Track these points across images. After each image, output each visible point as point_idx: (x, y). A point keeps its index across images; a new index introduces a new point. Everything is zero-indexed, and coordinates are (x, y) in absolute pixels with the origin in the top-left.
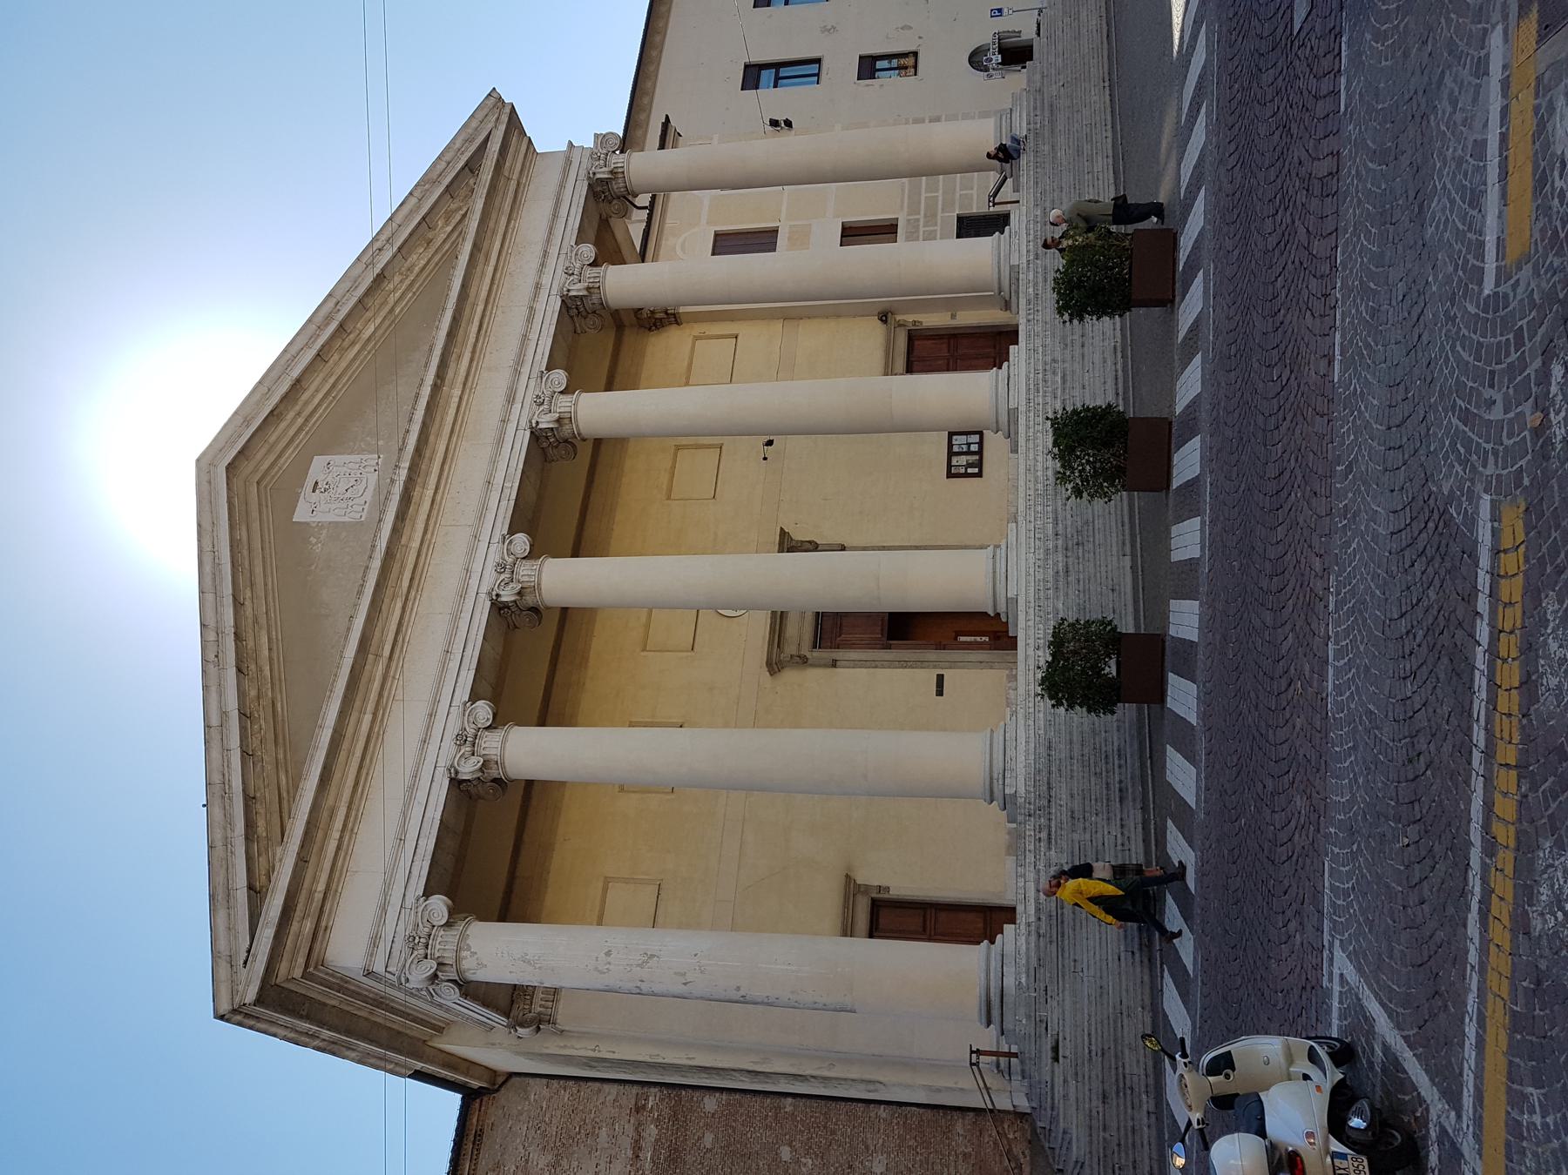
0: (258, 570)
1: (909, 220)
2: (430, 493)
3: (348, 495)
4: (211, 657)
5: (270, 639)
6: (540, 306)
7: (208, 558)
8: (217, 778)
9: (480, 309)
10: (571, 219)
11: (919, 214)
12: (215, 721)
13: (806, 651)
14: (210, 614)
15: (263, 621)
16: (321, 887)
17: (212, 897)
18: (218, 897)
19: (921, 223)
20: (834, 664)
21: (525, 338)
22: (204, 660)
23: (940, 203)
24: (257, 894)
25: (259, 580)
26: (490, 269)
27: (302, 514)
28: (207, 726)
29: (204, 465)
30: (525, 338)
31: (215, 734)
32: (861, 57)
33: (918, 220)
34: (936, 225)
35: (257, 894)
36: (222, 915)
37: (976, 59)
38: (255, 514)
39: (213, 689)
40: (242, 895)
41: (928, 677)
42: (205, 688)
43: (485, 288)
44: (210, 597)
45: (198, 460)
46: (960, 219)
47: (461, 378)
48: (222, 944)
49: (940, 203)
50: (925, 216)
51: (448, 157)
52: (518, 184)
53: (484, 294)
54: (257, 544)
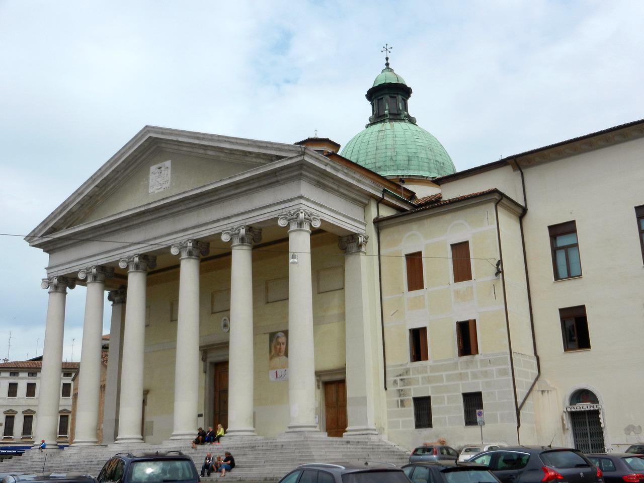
0: (131, 169)
1: (426, 367)
2: (150, 218)
3: (157, 183)
4: (94, 178)
5: (114, 187)
6: (221, 223)
7: (119, 155)
8: (67, 203)
9: (216, 198)
10: (261, 217)
11: (431, 372)
12: (79, 192)
13: (209, 360)
14: (104, 168)
15: (117, 181)
16: (59, 246)
17: (44, 221)
18: (45, 223)
19: (426, 375)
20: (205, 372)
21: (207, 224)
22: (91, 177)
23: (438, 384)
24: (54, 230)
25: (129, 170)
26: (233, 192)
27: (153, 168)
28: (77, 191)
29: (147, 129)
30: (207, 224)
31: (77, 194)
32: (583, 307)
33: (426, 372)
34: (423, 384)
35: (54, 230)
36: (41, 226)
37: (583, 395)
38: (148, 153)
39: (86, 185)
40: (48, 228)
41: (202, 412)
42: (85, 183)
43: (225, 195)
44: (108, 164)
45: (146, 126)
46: (428, 399)
47: (188, 206)
48: (36, 231)
49: (438, 384)
50: (428, 377)
51: (268, 145)
52: (277, 181)
53: (222, 196)
54: (139, 161)
